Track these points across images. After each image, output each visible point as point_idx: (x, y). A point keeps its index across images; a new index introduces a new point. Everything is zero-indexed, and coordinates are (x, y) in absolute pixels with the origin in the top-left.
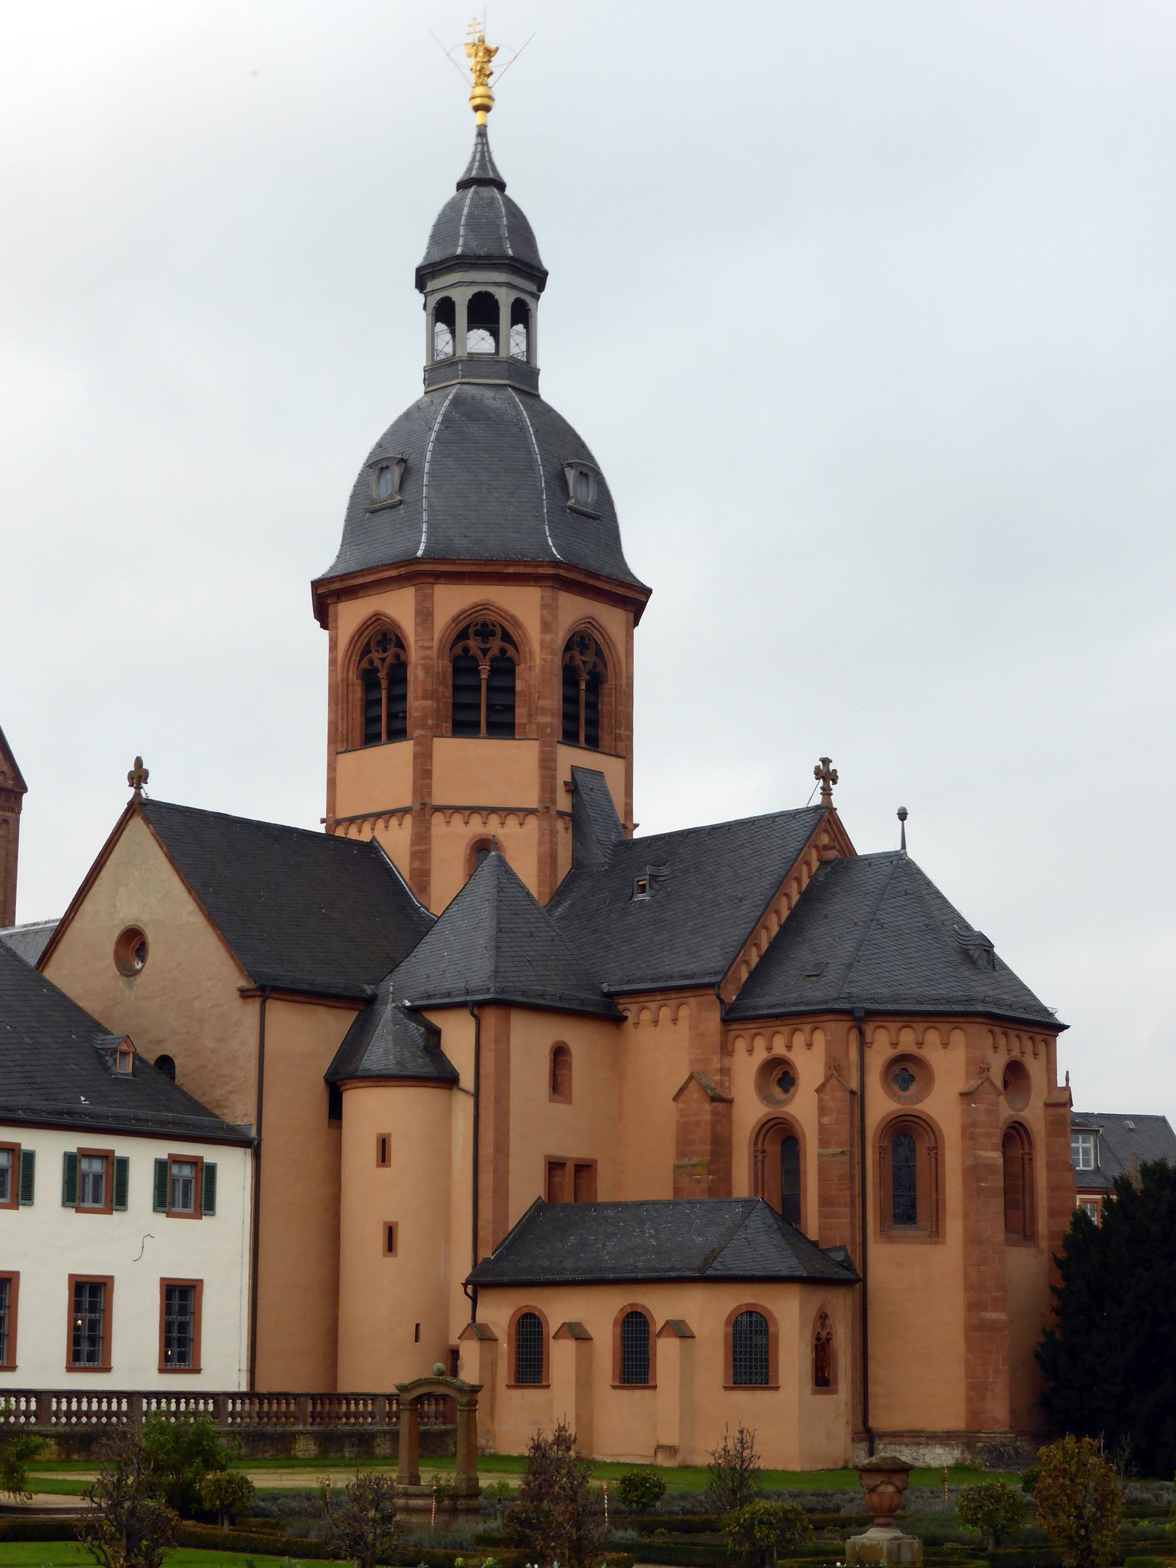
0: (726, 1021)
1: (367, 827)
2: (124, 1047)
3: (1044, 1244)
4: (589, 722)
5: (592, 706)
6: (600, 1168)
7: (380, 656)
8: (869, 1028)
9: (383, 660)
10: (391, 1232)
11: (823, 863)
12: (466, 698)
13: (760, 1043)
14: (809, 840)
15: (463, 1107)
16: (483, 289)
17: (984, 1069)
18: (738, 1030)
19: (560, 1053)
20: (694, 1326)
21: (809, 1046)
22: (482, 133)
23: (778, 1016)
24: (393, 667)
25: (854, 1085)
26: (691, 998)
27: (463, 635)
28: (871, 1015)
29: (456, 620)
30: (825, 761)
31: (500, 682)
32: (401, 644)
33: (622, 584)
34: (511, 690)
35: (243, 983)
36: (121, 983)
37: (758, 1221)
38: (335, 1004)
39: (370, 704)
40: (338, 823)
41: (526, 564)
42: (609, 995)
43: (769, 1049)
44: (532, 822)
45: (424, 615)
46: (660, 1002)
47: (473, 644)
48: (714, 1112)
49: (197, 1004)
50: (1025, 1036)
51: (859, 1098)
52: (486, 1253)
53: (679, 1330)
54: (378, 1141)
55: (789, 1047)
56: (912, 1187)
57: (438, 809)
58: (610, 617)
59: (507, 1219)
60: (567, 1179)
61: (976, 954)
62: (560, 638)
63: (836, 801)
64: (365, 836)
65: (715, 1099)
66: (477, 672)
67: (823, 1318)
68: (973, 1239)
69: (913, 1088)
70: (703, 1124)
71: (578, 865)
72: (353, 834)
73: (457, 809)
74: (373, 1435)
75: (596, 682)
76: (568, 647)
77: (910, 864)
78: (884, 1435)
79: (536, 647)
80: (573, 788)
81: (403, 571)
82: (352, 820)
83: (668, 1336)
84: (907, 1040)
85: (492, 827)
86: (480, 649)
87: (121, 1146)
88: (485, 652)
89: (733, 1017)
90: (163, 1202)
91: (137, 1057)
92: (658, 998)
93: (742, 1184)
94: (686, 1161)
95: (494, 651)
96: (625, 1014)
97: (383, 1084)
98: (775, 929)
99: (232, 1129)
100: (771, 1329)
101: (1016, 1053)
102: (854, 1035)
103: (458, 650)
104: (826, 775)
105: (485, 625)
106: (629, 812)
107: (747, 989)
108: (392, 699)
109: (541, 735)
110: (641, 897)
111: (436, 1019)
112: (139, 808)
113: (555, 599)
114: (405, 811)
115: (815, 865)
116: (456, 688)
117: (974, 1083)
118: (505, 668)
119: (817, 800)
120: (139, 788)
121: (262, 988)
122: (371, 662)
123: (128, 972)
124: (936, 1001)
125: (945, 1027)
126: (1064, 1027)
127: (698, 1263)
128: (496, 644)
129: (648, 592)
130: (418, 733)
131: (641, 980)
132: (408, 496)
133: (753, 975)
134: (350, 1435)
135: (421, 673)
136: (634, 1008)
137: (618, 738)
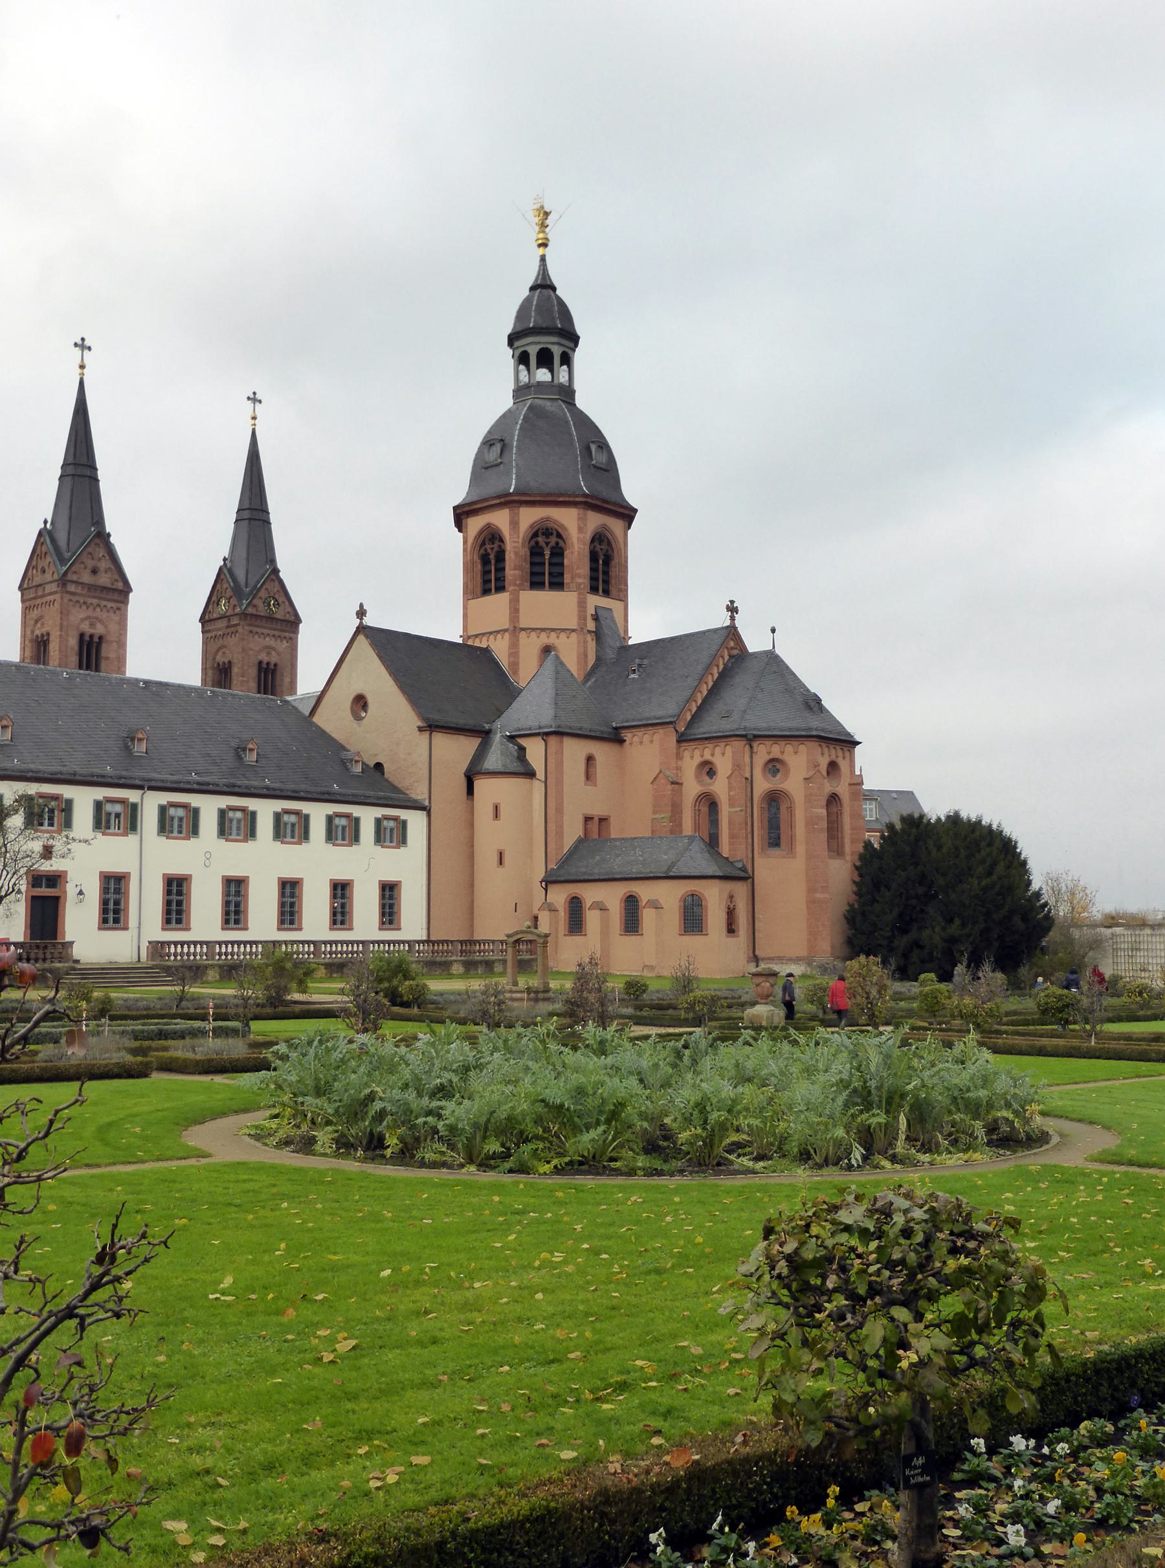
0: (678, 741)
1: (485, 639)
2: (357, 758)
3: (848, 858)
4: (604, 581)
5: (606, 573)
6: (612, 820)
8: (755, 744)
11: (731, 656)
12: (537, 569)
13: (697, 753)
14: (723, 644)
15: (538, 787)
17: (816, 766)
19: (590, 759)
20: (663, 902)
21: (723, 754)
23: (706, 739)
25: (748, 775)
27: (535, 535)
28: (756, 737)
29: (531, 526)
30: (732, 602)
31: (556, 560)
32: (501, 540)
33: (621, 506)
34: (562, 564)
35: (420, 724)
36: (355, 724)
37: (697, 848)
39: (486, 573)
40: (469, 637)
41: (569, 496)
42: (616, 729)
43: (702, 756)
44: (574, 635)
45: (514, 524)
47: (541, 539)
48: (673, 790)
50: (838, 748)
51: (750, 781)
52: (549, 867)
53: (655, 905)
55: (713, 755)
56: (778, 828)
58: (615, 525)
59: (562, 847)
60: (594, 826)
61: (812, 704)
62: (588, 536)
63: (738, 623)
64: (484, 645)
65: (672, 783)
66: (543, 555)
67: (731, 897)
68: (810, 856)
69: (779, 776)
71: (599, 659)
72: (477, 644)
73: (533, 629)
74: (493, 962)
75: (608, 560)
76: (593, 541)
77: (777, 656)
78: (763, 959)
79: (575, 541)
80: (596, 618)
81: (502, 500)
82: (476, 636)
84: (776, 750)
85: (552, 639)
87: (356, 811)
88: (547, 544)
89: (682, 739)
90: (379, 839)
91: (363, 763)
93: (688, 827)
94: (657, 816)
95: (553, 544)
98: (705, 693)
99: (416, 801)
101: (833, 757)
102: (747, 747)
103: (533, 542)
104: (732, 609)
105: (547, 529)
106: (626, 631)
107: (690, 725)
108: (496, 570)
109: (578, 588)
110: (633, 676)
111: (523, 742)
112: (361, 629)
113: (585, 515)
114: (506, 630)
115: (727, 658)
116: (532, 564)
117: (811, 773)
118: (558, 553)
119: (728, 623)
120: (361, 619)
121: (430, 726)
123: (358, 718)
124: (790, 729)
125: (795, 743)
126: (859, 743)
127: (665, 869)
128: (553, 540)
129: (636, 511)
130: (511, 588)
131: (633, 720)
132: (505, 459)
133: (693, 717)
134: (481, 962)
135: (512, 555)
137: (620, 590)
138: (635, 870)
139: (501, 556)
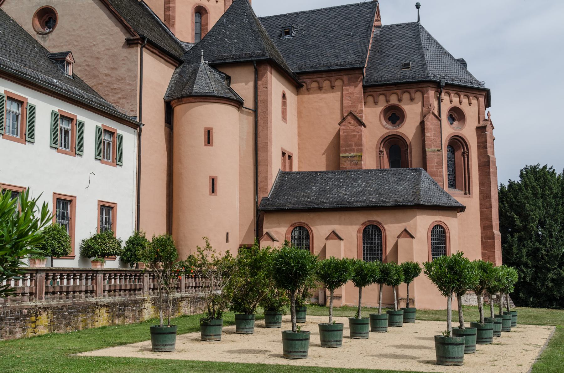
10: (213, 181)
18: (370, 92)
26: (344, 76)
38: (168, 60)
46: (325, 78)
49: (94, 48)
52: (261, 196)
54: (205, 132)
70: (357, 136)
83: (404, 237)
90: (98, 155)
92: (324, 76)
96: (303, 84)
97: (208, 100)
100: (447, 234)
110: (287, 37)
111: (229, 72)
136: (308, 81)
138: (373, 199)
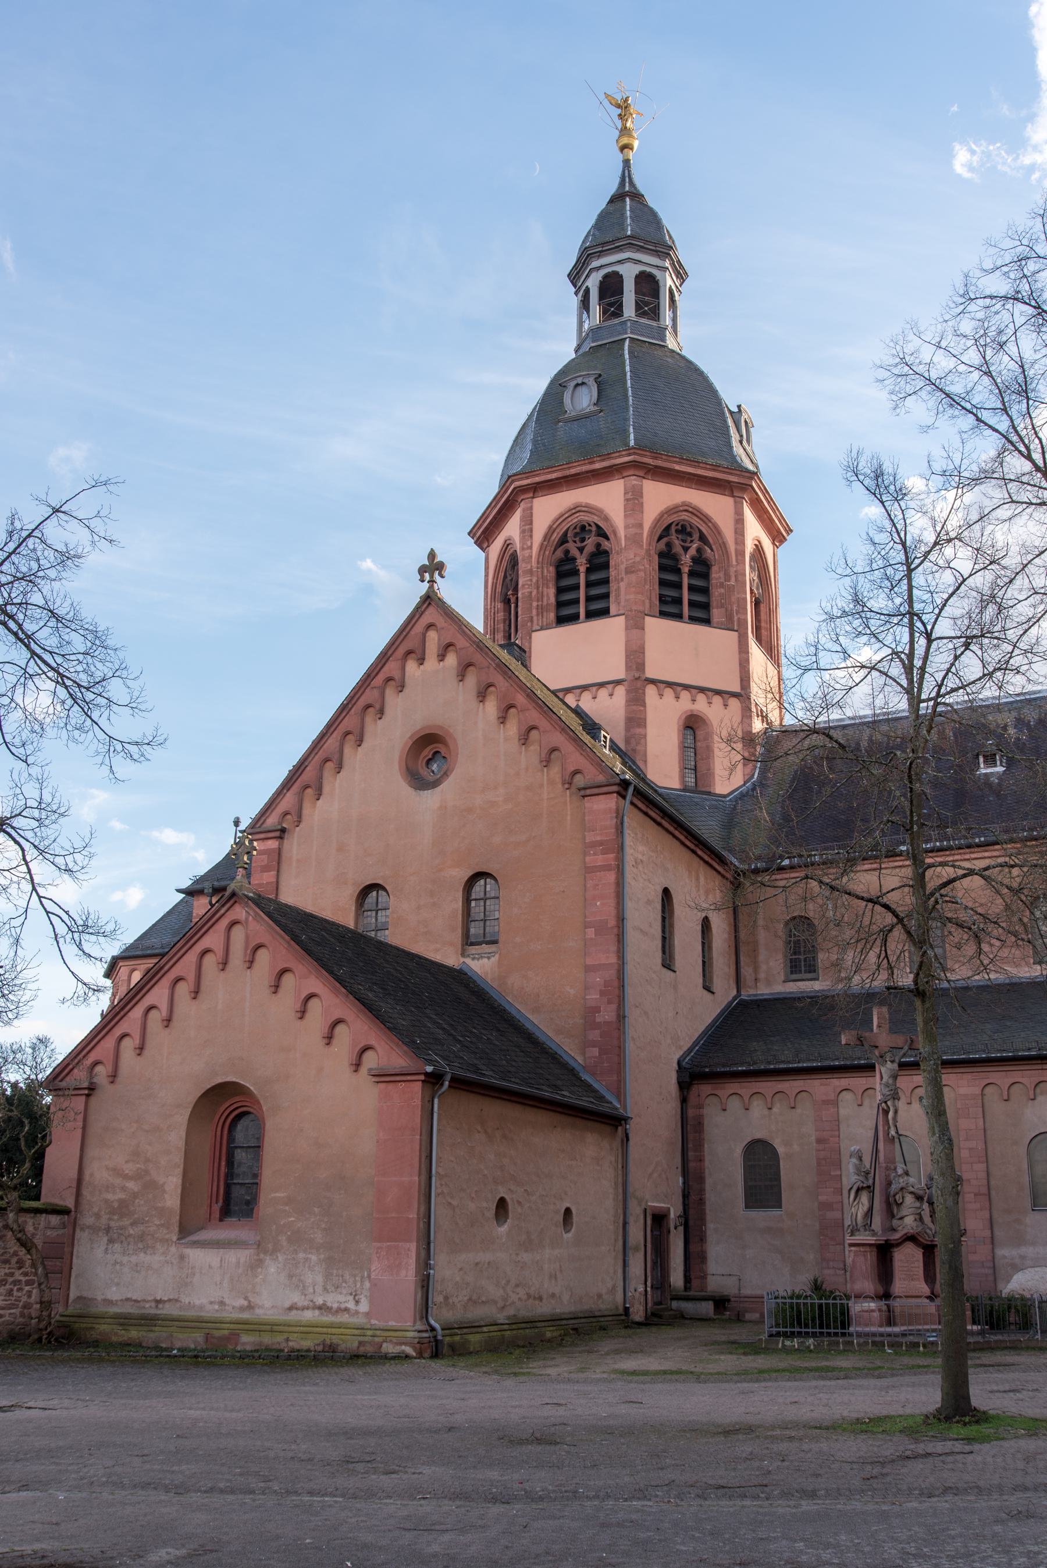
7: (579, 545)
9: (581, 550)
16: (648, 269)
22: (627, 163)
24: (592, 556)
57: (653, 682)
85: (701, 705)
86: (682, 546)
114: (618, 682)
122: (567, 552)
139: (600, 561)
